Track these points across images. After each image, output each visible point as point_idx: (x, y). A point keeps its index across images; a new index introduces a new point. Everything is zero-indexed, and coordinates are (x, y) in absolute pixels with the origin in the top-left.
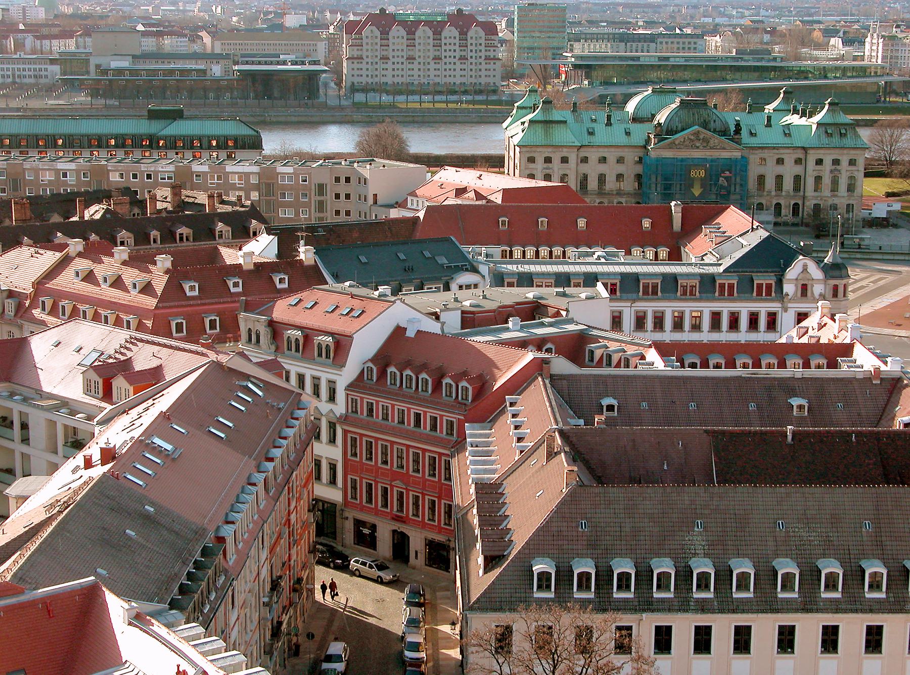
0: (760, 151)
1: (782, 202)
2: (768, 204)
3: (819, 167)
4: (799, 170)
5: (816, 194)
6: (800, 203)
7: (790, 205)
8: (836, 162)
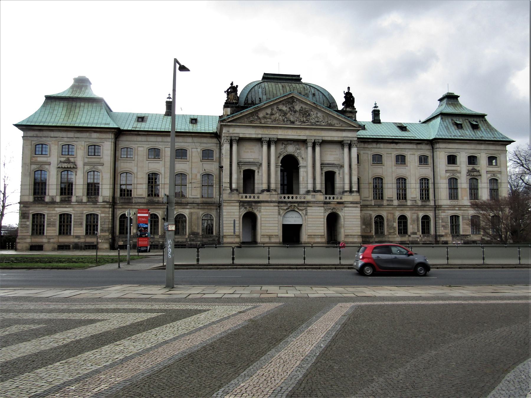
0: (374, 145)
1: (408, 214)
2: (390, 217)
3: (452, 167)
4: (426, 172)
5: (454, 202)
6: (431, 214)
7: (418, 218)
8: (472, 160)
